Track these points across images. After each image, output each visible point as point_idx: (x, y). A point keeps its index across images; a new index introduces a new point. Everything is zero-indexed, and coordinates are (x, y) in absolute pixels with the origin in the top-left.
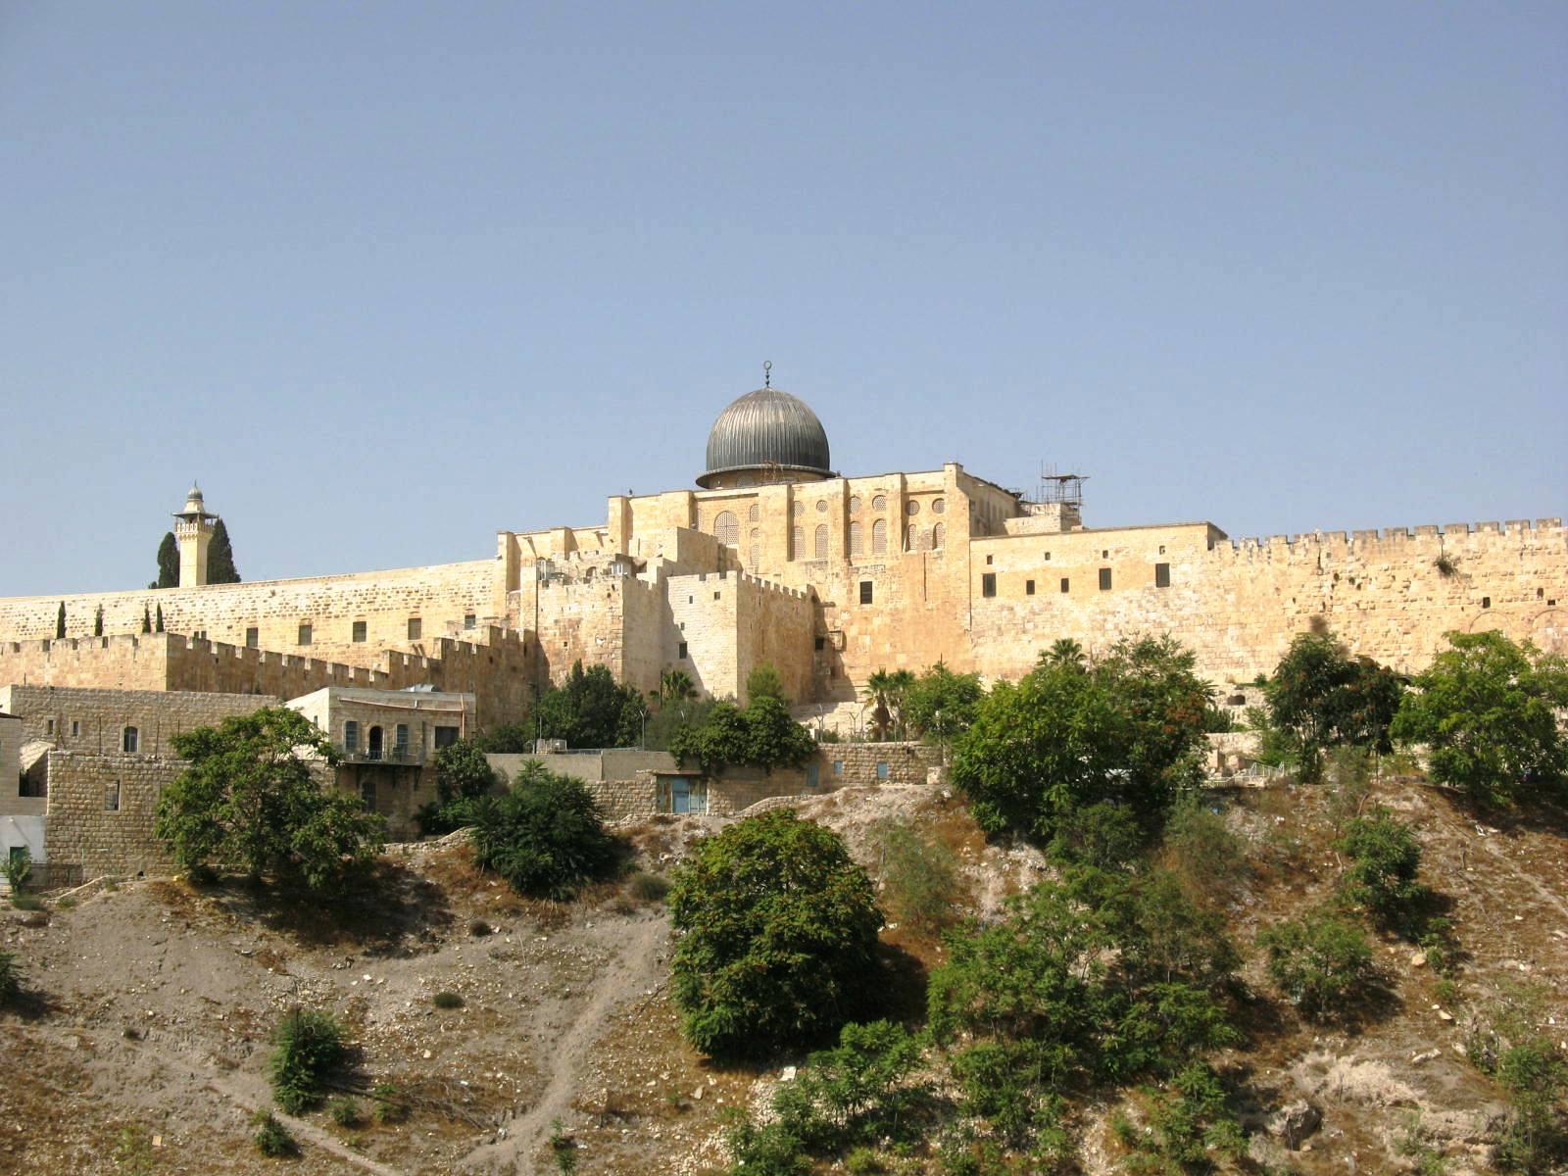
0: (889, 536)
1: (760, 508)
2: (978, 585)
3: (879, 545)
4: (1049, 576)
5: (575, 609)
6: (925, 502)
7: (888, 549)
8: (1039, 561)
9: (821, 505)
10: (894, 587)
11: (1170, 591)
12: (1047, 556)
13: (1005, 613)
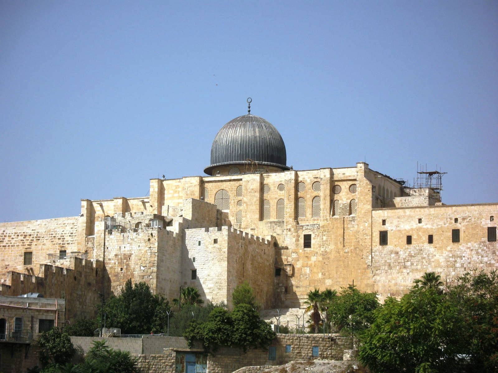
0: (322, 207)
2: (377, 238)
3: (315, 212)
6: (344, 186)
7: (321, 215)
9: (281, 187)
10: (325, 238)
13: (393, 255)
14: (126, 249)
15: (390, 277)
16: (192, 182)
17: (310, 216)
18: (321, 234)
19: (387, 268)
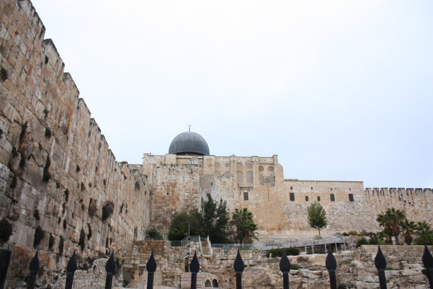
0: (254, 177)
2: (288, 197)
4: (313, 195)
6: (266, 167)
8: (309, 190)
11: (354, 203)
12: (312, 188)
13: (298, 207)
14: (172, 179)
15: (298, 219)
17: (246, 182)
18: (254, 193)
19: (295, 214)
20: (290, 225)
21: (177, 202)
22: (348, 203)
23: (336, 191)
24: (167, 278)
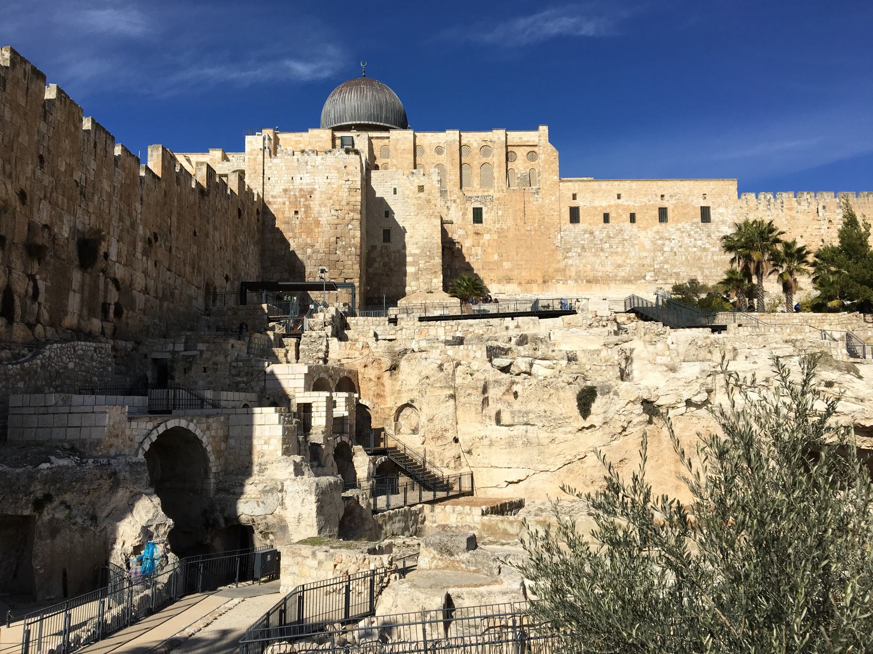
0: (496, 175)
1: (391, 148)
2: (567, 215)
3: (486, 182)
4: (620, 211)
5: (307, 179)
6: (521, 153)
8: (614, 201)
9: (439, 150)
10: (500, 213)
11: (711, 226)
12: (619, 197)
13: (587, 236)
14: (304, 181)
16: (321, 135)
17: (478, 187)
19: (579, 251)
20: (568, 273)
21: (316, 230)
22: (698, 227)
23: (673, 201)
24: (238, 375)
